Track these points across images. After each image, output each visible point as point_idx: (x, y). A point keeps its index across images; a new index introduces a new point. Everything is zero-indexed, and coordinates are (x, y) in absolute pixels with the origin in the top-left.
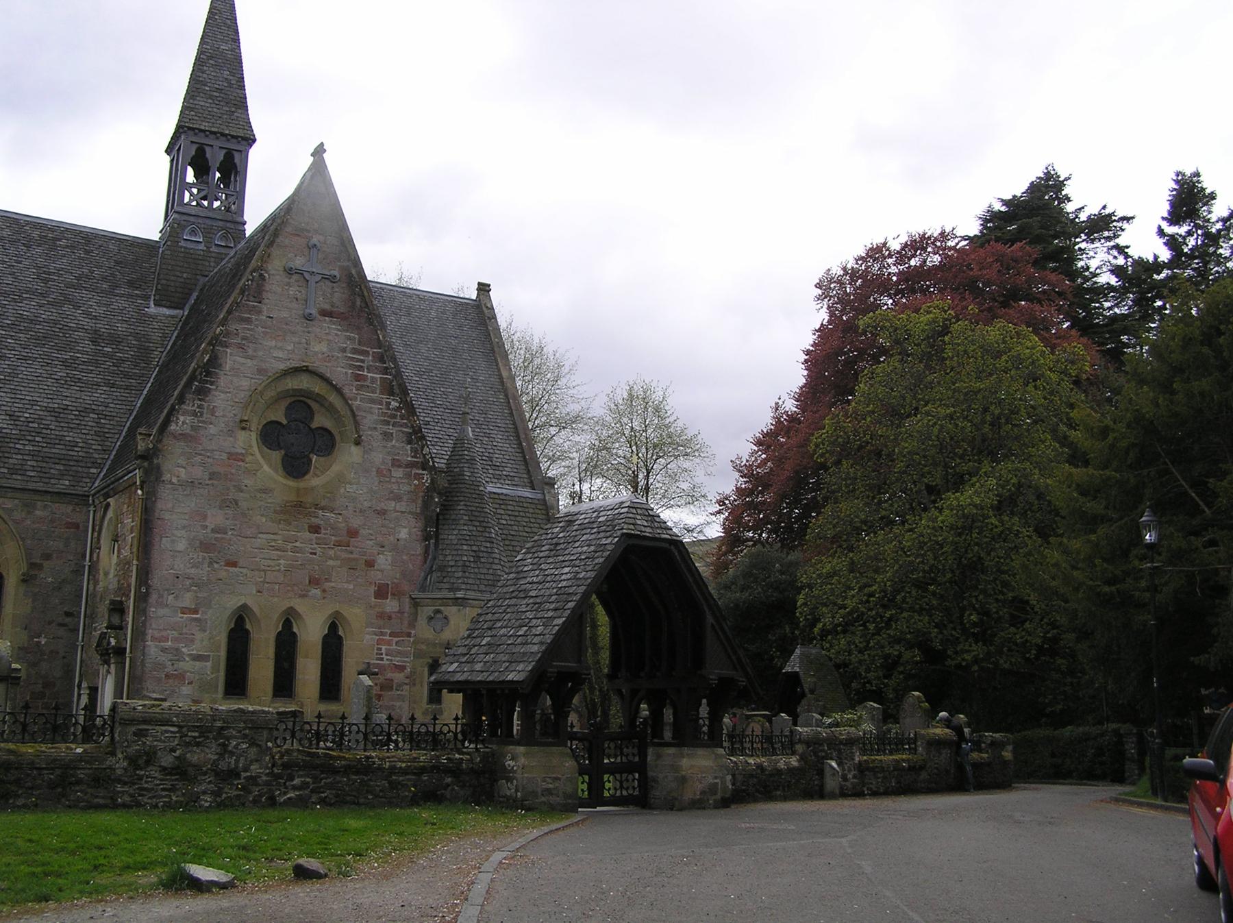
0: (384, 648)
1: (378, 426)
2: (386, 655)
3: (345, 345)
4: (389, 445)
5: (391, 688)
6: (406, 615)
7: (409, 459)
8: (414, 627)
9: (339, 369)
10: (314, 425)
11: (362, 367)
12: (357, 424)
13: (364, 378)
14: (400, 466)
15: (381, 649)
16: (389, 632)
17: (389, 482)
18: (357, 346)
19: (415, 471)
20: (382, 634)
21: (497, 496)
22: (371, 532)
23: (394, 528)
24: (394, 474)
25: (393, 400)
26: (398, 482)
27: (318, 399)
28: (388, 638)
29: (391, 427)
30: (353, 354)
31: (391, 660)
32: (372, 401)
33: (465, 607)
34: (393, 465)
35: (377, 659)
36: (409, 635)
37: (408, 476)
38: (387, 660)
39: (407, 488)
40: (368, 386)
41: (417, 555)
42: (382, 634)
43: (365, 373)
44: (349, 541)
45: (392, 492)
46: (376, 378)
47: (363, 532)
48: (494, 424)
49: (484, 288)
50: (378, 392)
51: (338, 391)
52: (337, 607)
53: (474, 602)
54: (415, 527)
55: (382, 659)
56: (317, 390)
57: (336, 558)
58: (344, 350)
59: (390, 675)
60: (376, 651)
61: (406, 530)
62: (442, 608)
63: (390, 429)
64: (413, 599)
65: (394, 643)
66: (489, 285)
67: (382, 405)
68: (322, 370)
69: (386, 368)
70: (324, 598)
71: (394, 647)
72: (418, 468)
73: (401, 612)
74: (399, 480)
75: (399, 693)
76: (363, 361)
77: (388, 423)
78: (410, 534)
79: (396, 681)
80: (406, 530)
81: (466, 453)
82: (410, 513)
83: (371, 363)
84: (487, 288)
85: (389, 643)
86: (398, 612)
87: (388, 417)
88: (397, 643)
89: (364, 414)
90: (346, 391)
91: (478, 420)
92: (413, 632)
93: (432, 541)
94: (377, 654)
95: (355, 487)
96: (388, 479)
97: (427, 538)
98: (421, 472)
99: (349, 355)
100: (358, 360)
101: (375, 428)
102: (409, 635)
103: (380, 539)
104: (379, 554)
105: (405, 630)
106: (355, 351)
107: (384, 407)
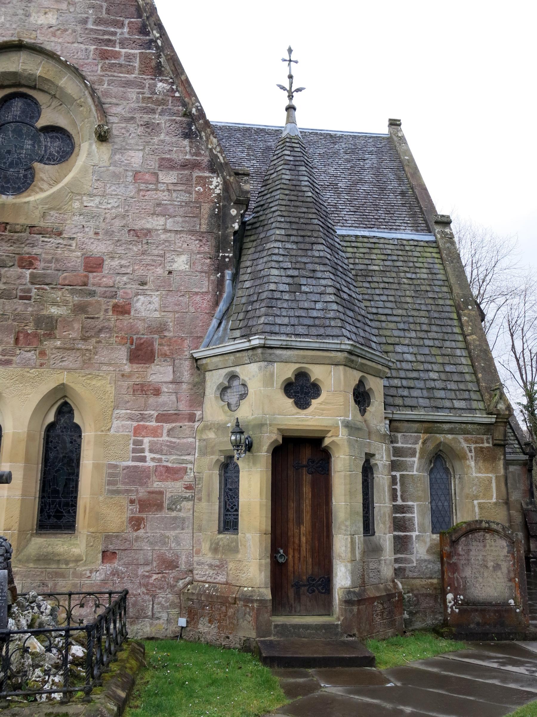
0: (146, 440)
1: (137, 116)
2: (151, 451)
3: (86, 15)
4: (156, 140)
5: (159, 507)
6: (184, 386)
7: (187, 157)
8: (201, 404)
9: (76, 45)
10: (41, 123)
11: (109, 40)
12: (103, 112)
13: (116, 55)
14: (172, 168)
15: (141, 443)
16: (155, 413)
17: (156, 190)
18: (104, 15)
19: (197, 173)
20: (143, 418)
21: (366, 240)
22: (123, 262)
23: (163, 256)
24: (162, 176)
25: (161, 81)
26: (168, 190)
27: (46, 88)
28: (154, 424)
29: (157, 116)
30: (97, 25)
31: (160, 460)
32: (128, 84)
33: (272, 362)
34: (161, 167)
35: (135, 459)
36: (192, 418)
37: (187, 181)
38: (153, 459)
39: (185, 197)
40: (121, 65)
41: (202, 293)
42: (143, 418)
43: (117, 49)
44: (87, 277)
45: (159, 205)
46: (134, 55)
47: (110, 264)
48: (401, 221)
49: (394, 123)
50: (137, 72)
51: (76, 71)
52: (64, 378)
53: (284, 352)
54: (199, 253)
55: (143, 459)
56: (38, 73)
57: (66, 303)
58: (85, 21)
59: (157, 485)
60: (131, 446)
61: (184, 258)
62: (238, 369)
63: (157, 119)
64: (197, 360)
65: (165, 432)
66: (399, 121)
67: (143, 88)
68: (48, 47)
69: (151, 41)
70: (41, 365)
71: (165, 438)
72: (202, 169)
73: (176, 382)
74: (171, 187)
75: (174, 514)
76: (114, 34)
77: (153, 111)
78: (192, 263)
79: (168, 495)
80: (184, 258)
81: (288, 152)
82: (192, 232)
83: (127, 36)
84: (398, 123)
85: (155, 432)
86: (171, 383)
87: (153, 102)
88: (170, 432)
89: (114, 101)
90: (86, 71)
91: (384, 219)
92: (198, 413)
93: (228, 273)
94: (134, 451)
95: (97, 200)
96: (151, 186)
97: (220, 267)
98: (207, 174)
99: (92, 27)
100: (105, 33)
101: (132, 118)
102: (192, 418)
103: (140, 271)
104: (137, 294)
105: (183, 407)
106: (99, 21)
107: (146, 90)
